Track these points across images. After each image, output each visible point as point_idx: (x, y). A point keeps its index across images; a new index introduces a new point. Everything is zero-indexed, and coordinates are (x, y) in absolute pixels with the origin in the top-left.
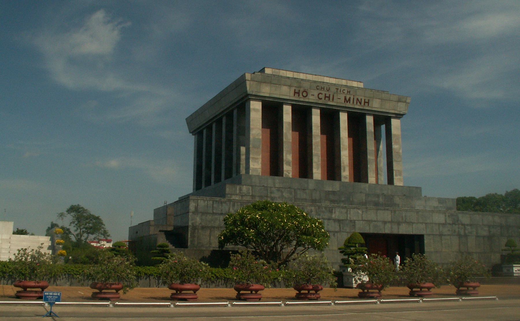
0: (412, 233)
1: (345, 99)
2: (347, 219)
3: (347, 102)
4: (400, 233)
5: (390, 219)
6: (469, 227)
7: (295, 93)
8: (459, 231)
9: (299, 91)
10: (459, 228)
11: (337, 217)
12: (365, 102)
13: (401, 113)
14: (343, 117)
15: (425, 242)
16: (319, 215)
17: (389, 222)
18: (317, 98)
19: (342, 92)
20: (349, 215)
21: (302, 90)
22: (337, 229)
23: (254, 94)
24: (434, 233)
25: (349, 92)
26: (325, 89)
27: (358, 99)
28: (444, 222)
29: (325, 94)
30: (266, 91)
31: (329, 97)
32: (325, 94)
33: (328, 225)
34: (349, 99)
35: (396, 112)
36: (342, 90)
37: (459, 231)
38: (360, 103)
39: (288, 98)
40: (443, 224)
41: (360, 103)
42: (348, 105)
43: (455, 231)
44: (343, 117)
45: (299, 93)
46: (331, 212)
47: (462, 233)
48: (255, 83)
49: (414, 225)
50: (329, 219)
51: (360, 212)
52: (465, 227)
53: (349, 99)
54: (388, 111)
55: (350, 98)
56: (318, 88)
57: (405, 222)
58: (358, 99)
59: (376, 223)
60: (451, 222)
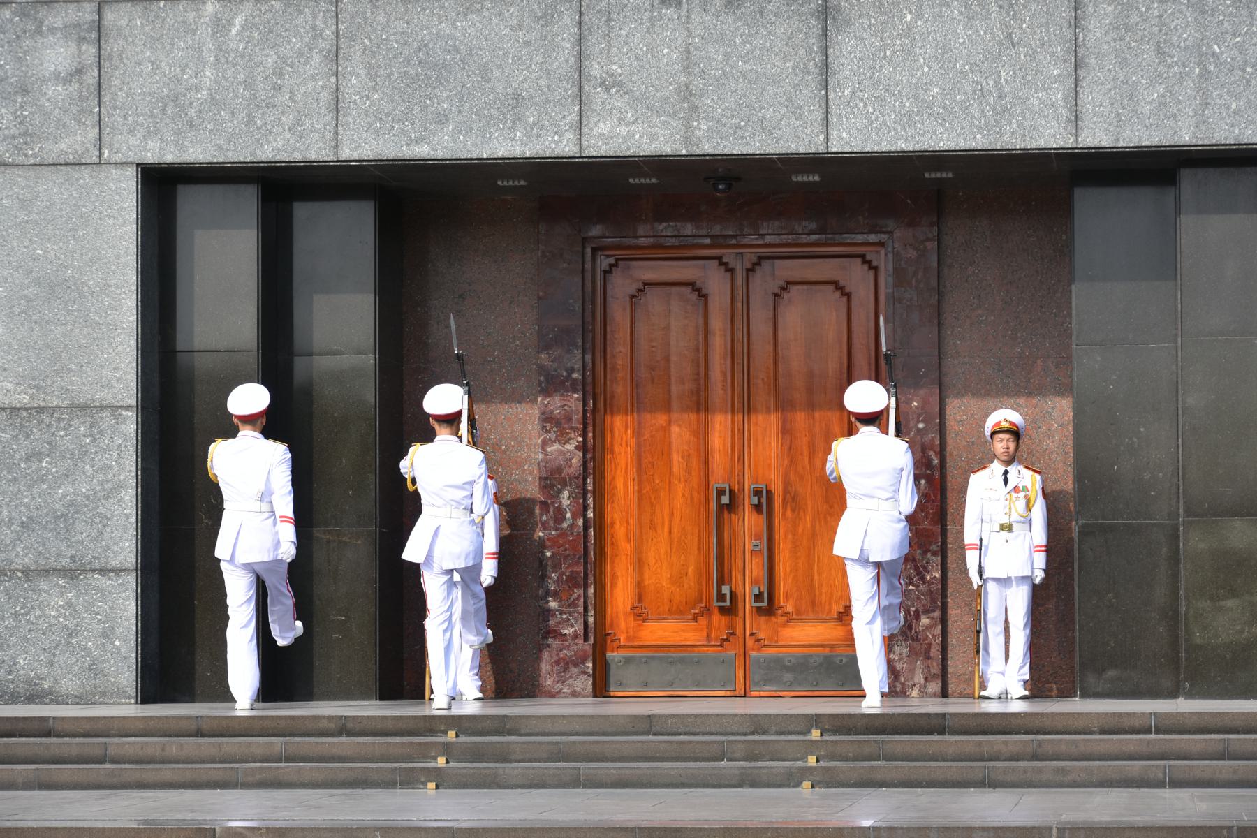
0: (1050, 134)
4: (847, 139)
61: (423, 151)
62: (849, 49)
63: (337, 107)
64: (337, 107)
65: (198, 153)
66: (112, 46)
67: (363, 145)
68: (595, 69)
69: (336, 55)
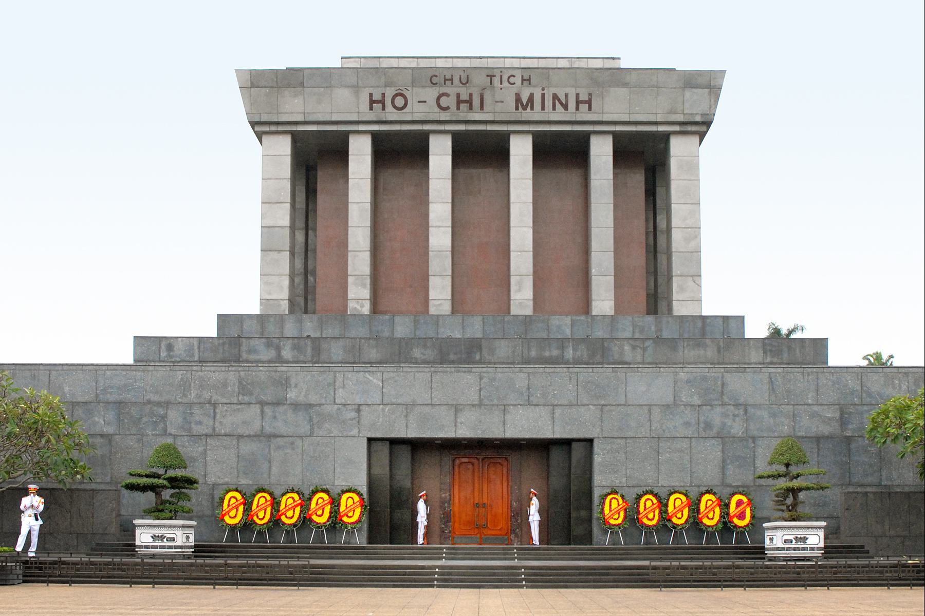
0: (548, 434)
1: (518, 99)
2: (335, 403)
3: (525, 108)
5: (475, 398)
6: (765, 414)
7: (372, 102)
8: (724, 424)
9: (383, 94)
10: (725, 415)
11: (302, 399)
12: (578, 102)
13: (698, 119)
14: (521, 151)
15: (597, 459)
16: (251, 394)
17: (473, 405)
18: (437, 109)
19: (506, 84)
20: (340, 392)
21: (390, 92)
22: (305, 428)
23: (265, 118)
24: (630, 434)
25: (526, 81)
26: (456, 81)
27: (555, 97)
28: (670, 399)
29: (458, 95)
30: (294, 107)
31: (470, 102)
32: (458, 95)
33: (275, 417)
34: (531, 99)
35: (680, 118)
36: (505, 78)
37: (724, 424)
38: (565, 107)
39: (354, 118)
40: (668, 406)
41: (565, 107)
42: (527, 115)
43: (708, 425)
44: (521, 151)
45: (382, 102)
46: (285, 383)
47: (737, 429)
48: (263, 90)
49: (558, 411)
50: (278, 404)
51: (375, 380)
52: (746, 411)
53: (531, 99)
54: (652, 118)
55: (532, 96)
56: (435, 80)
57: (530, 404)
58: (555, 97)
59: (427, 409)
60: (696, 401)
61: (424, 436)
62: (508, 417)
63: (407, 426)
64: (407, 426)
65: (378, 435)
66: (362, 413)
67: (413, 433)
68: (458, 420)
69: (406, 416)
